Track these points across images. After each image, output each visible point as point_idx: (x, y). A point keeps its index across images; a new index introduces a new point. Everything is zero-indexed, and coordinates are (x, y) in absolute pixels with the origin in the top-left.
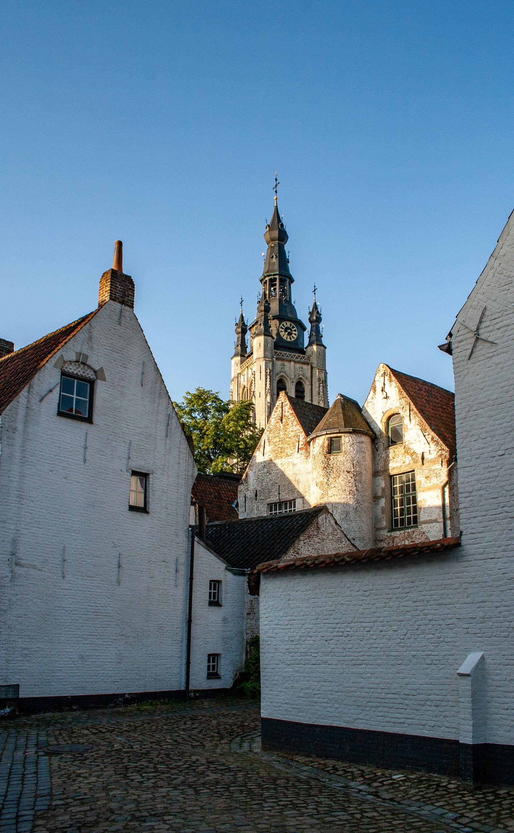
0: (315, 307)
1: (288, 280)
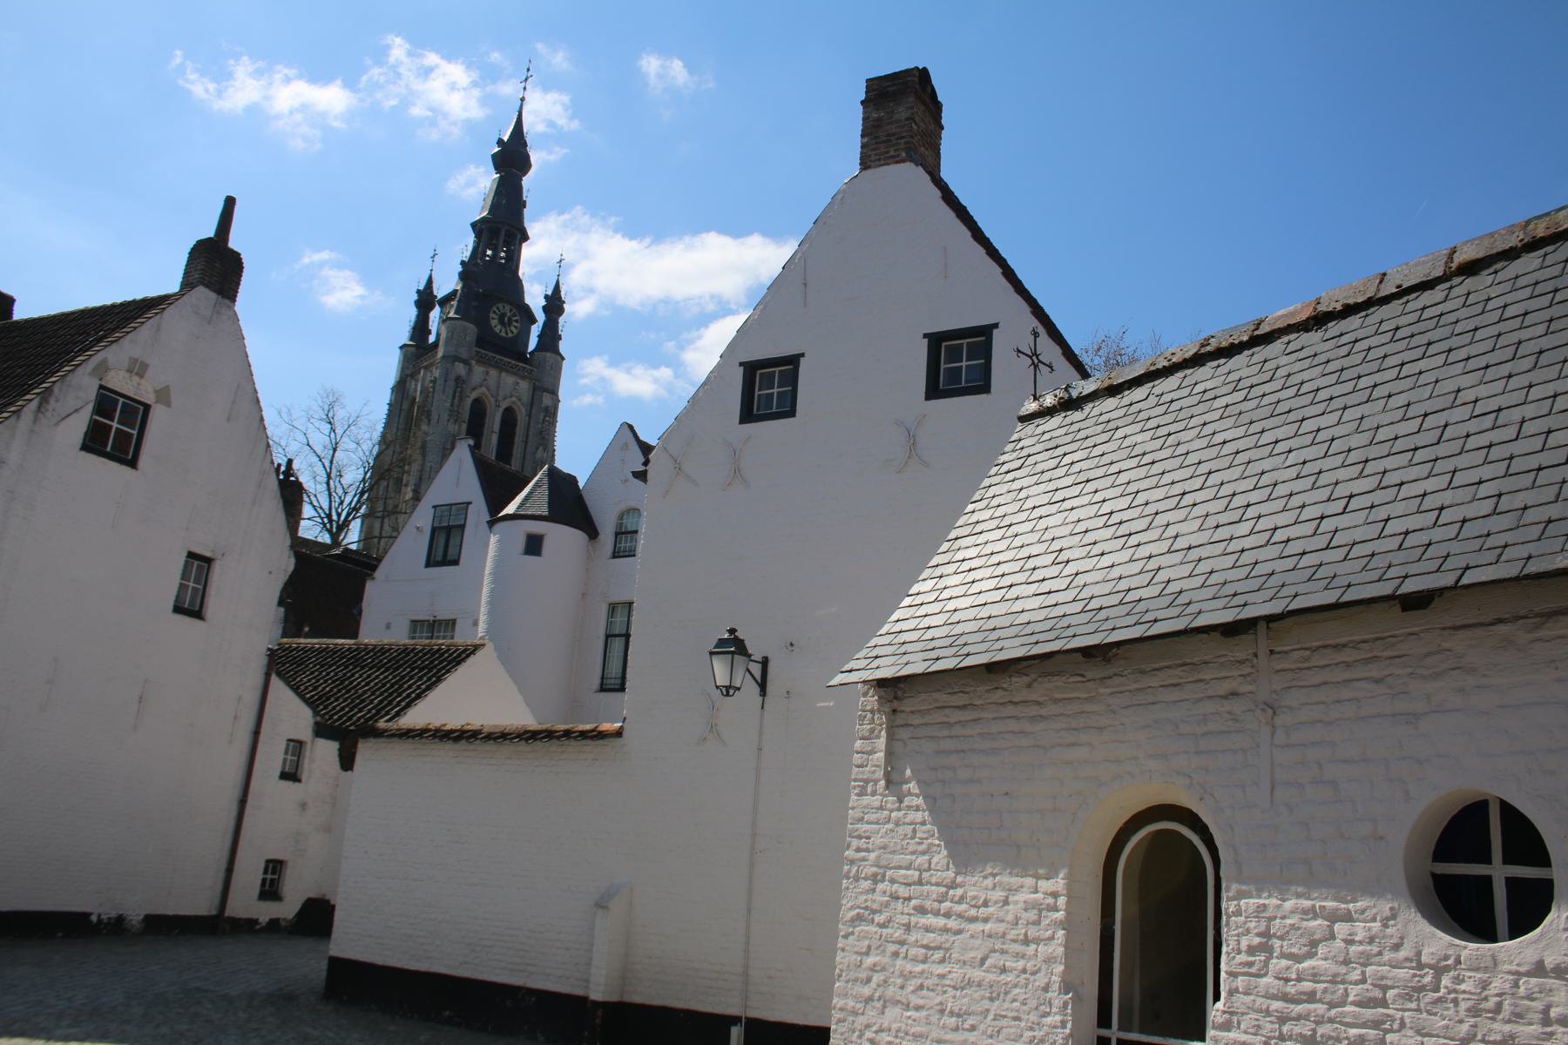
0: (557, 289)
1: (519, 236)
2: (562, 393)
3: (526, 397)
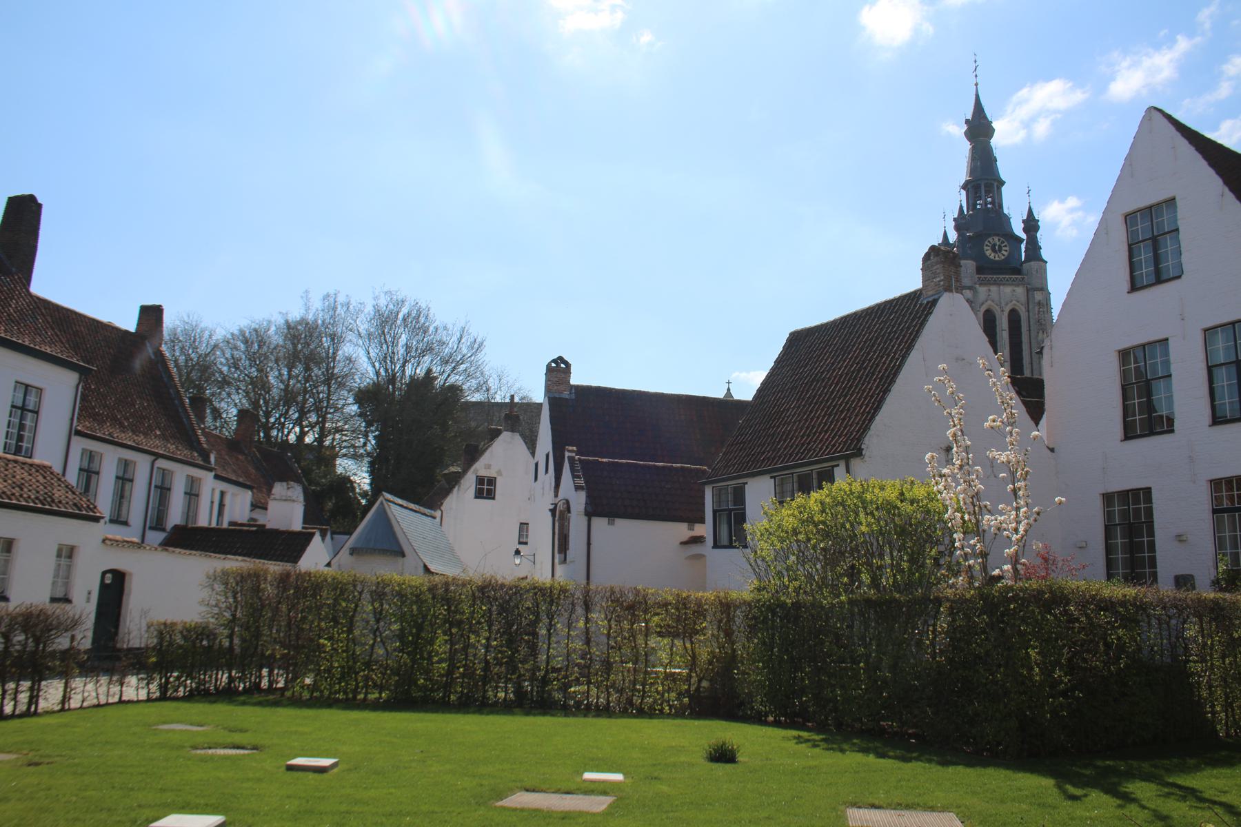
0: (1030, 212)
1: (996, 184)
2: (1050, 289)
3: (1023, 299)
